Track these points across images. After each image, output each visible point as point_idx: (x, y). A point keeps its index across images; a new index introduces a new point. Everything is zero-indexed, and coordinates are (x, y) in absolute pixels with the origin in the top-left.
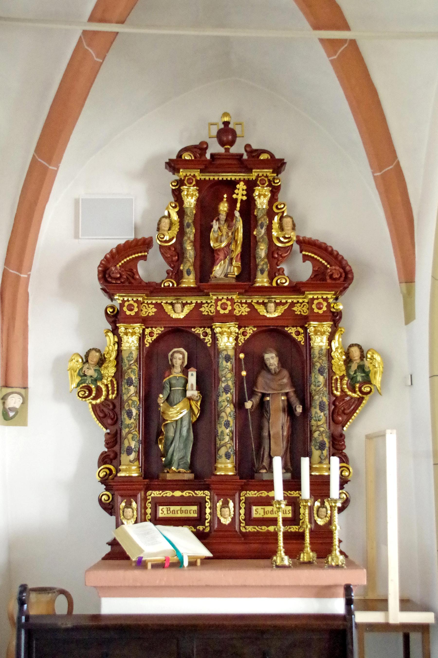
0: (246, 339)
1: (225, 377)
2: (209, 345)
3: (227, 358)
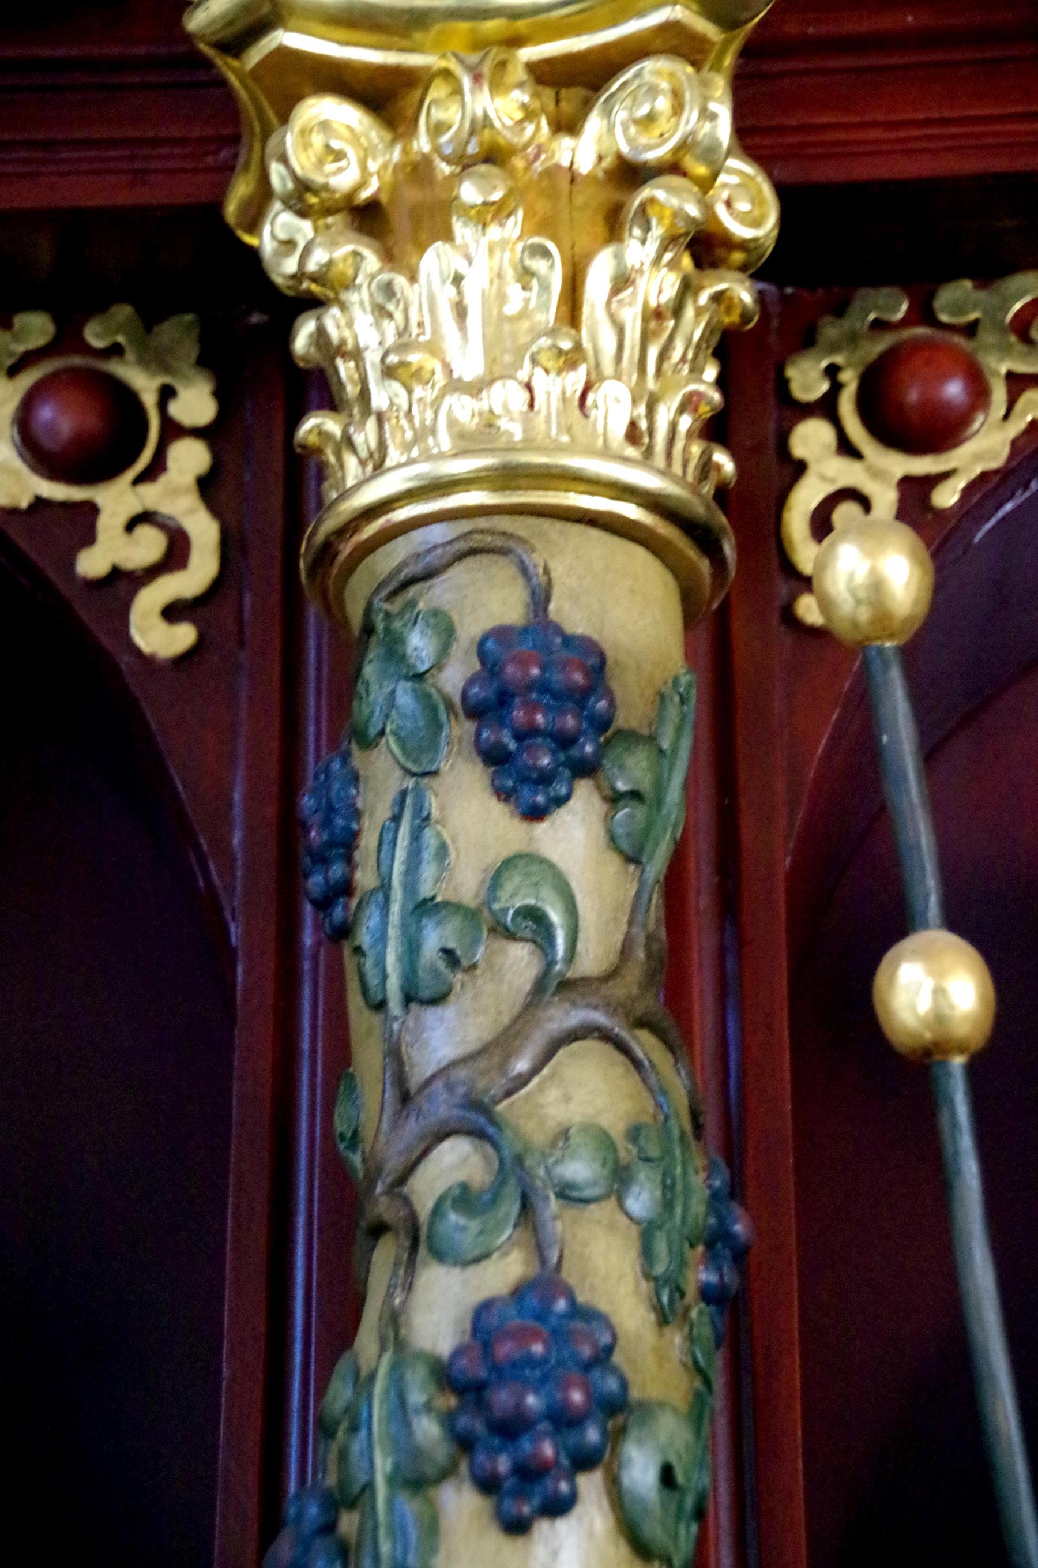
0: (947, 497)
1: (479, 1121)
2: (157, 635)
3: (539, 719)
